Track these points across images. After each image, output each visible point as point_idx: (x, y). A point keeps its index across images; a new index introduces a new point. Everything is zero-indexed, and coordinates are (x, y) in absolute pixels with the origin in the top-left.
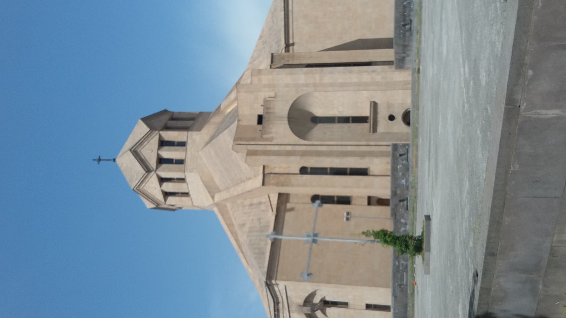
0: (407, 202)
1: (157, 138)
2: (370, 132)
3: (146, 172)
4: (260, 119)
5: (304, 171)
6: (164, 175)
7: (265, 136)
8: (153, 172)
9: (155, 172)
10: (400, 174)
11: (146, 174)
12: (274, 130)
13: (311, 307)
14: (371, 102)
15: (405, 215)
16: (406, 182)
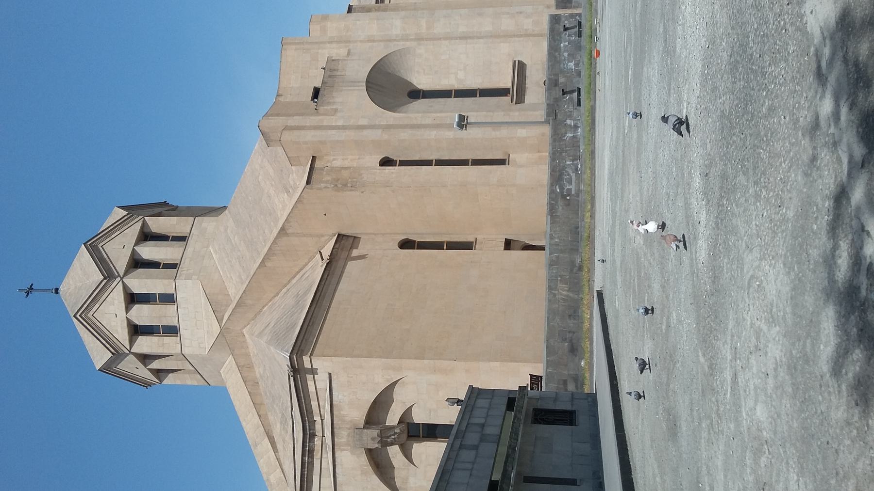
0: (579, 95)
3: (105, 278)
4: (316, 93)
5: (386, 162)
6: (135, 291)
7: (322, 109)
8: (119, 279)
9: (122, 279)
10: (566, 54)
11: (105, 281)
12: (339, 99)
13: (381, 430)
14: (515, 62)
15: (575, 114)
16: (577, 65)
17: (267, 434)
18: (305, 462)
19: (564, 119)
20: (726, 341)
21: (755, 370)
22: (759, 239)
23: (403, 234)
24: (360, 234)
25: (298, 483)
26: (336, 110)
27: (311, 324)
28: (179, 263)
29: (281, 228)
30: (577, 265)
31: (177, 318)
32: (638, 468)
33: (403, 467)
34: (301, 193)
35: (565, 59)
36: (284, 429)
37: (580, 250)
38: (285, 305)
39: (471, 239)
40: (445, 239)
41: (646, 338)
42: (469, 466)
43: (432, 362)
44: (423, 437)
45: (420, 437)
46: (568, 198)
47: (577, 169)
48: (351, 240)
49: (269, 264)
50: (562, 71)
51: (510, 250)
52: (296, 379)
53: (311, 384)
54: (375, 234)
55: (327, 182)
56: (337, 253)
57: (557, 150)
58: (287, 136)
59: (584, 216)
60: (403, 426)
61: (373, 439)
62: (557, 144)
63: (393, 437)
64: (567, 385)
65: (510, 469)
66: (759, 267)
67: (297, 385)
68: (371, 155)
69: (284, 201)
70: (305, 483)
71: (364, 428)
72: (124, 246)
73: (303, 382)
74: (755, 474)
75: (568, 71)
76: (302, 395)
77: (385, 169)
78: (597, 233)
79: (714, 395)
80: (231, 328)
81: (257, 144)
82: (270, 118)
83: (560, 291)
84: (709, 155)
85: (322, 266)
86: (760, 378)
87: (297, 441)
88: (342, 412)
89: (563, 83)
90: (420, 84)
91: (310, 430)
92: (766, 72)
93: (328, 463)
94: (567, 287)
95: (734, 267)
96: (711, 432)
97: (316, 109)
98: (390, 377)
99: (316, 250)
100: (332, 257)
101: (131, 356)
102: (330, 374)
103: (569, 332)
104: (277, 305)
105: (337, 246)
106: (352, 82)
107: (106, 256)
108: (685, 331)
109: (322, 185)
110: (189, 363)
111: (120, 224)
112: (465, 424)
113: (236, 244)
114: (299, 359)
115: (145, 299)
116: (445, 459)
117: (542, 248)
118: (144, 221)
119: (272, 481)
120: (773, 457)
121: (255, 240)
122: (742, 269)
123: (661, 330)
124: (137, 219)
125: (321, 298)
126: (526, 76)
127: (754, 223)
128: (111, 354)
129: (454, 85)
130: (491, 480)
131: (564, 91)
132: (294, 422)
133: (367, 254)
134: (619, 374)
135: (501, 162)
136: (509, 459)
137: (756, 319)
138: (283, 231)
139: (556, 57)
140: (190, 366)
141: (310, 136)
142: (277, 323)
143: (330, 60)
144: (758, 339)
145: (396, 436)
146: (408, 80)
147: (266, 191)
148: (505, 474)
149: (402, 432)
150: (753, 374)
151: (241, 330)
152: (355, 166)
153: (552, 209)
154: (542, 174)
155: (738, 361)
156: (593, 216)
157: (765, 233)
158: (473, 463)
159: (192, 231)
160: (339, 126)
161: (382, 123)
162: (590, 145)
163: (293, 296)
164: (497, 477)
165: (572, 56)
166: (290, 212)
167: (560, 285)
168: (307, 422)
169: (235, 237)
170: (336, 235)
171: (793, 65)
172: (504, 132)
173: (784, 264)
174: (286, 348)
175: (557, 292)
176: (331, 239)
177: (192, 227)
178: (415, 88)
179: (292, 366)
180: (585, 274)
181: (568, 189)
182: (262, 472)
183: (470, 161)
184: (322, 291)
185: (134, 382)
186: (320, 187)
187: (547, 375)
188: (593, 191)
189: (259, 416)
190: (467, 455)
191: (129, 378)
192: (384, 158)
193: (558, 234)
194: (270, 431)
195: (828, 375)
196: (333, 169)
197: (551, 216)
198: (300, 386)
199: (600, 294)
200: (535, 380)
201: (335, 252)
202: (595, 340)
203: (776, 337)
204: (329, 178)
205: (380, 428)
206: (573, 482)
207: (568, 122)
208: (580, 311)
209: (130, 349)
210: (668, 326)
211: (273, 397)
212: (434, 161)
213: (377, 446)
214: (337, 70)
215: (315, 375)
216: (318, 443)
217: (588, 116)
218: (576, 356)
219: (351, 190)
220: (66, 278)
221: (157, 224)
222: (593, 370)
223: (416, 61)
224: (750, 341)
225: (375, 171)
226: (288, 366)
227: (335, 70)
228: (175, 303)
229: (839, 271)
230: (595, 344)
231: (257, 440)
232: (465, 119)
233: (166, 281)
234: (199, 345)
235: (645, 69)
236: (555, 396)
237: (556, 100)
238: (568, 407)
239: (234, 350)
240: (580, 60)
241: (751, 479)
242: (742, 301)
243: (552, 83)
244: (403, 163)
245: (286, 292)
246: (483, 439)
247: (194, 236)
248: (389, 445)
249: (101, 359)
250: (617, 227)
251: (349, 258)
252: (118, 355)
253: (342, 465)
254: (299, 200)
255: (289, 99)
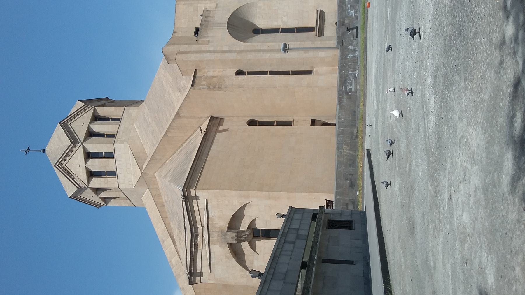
0: (357, 31)
1: (91, 112)
2: (316, 35)
3: (72, 143)
4: (197, 31)
5: (239, 73)
6: (91, 150)
7: (200, 40)
9: (82, 144)
10: (349, 6)
11: (72, 145)
13: (237, 233)
14: (318, 11)
15: (355, 43)
16: (356, 12)
17: (170, 235)
18: (193, 252)
19: (348, 46)
20: (445, 176)
21: (462, 192)
22: (467, 114)
23: (249, 116)
24: (225, 116)
25: (188, 263)
26: (209, 41)
27: (195, 170)
28: (116, 134)
29: (177, 113)
30: (355, 134)
31: (115, 167)
32: (390, 254)
33: (250, 254)
34: (189, 92)
35: (348, 9)
36: (180, 232)
37: (357, 125)
38: (179, 159)
39: (290, 119)
40: (275, 119)
41: (396, 177)
42: (290, 253)
43: (267, 192)
44: (262, 237)
45: (260, 237)
46: (350, 94)
47: (355, 77)
48: (219, 120)
49: (169, 135)
50: (347, 16)
51: (314, 126)
52: (187, 203)
53: (195, 205)
54: (233, 117)
55: (204, 85)
56: (210, 128)
57: (343, 65)
58: (179, 57)
59: (359, 105)
60: (250, 230)
61: (232, 238)
62: (344, 61)
63: (244, 237)
64: (348, 206)
65: (314, 255)
66: (466, 130)
67: (187, 206)
68: (230, 69)
69: (178, 96)
70: (193, 263)
71: (227, 231)
72: (83, 124)
73: (190, 204)
74: (461, 254)
75: (351, 16)
76: (190, 212)
77: (239, 77)
78: (367, 115)
79: (437, 209)
80: (148, 173)
81: (162, 62)
82: (169, 46)
83: (344, 150)
84: (437, 63)
85: (201, 136)
86: (465, 197)
87: (188, 239)
88: (214, 222)
89: (347, 23)
90: (260, 25)
91: (195, 233)
92: (473, 11)
93: (206, 252)
94: (349, 148)
95: (451, 131)
96: (435, 230)
97: (197, 41)
98: (242, 202)
99: (197, 126)
100: (207, 130)
101: (89, 190)
102: (207, 200)
103: (350, 175)
104: (175, 159)
105: (210, 124)
106: (219, 24)
107: (72, 130)
108: (420, 171)
109: (201, 87)
110: (123, 193)
111: (80, 111)
112: (287, 228)
113: (150, 123)
114: (188, 191)
115: (96, 155)
116: (275, 249)
117: (334, 125)
118: (95, 108)
119: (173, 263)
120: (472, 244)
121: (161, 120)
122: (456, 132)
123: (406, 172)
124: (90, 108)
125: (201, 155)
126: (324, 20)
127: (464, 104)
128: (76, 188)
129: (281, 26)
130: (302, 261)
131: (348, 28)
132: (186, 228)
133: (229, 129)
134: (380, 199)
135: (309, 72)
136: (314, 249)
137: (464, 162)
138: (178, 115)
139: (343, 8)
140: (124, 195)
141: (193, 57)
142: (175, 169)
143: (206, 11)
144: (465, 173)
145: (246, 236)
146: (253, 22)
147: (167, 91)
148: (311, 258)
149: (250, 234)
150: (461, 195)
151: (153, 174)
152: (221, 75)
153: (340, 101)
154: (334, 79)
155: (453, 187)
156: (365, 105)
157: (470, 110)
158: (292, 251)
159: (123, 115)
160: (211, 51)
161: (237, 49)
162: (363, 61)
163: (184, 154)
164: (306, 259)
165: (353, 7)
166: (182, 103)
167: (344, 147)
168: (193, 228)
169: (149, 119)
170: (210, 118)
171: (489, 6)
172: (311, 54)
173: (482, 128)
174: (181, 184)
175: (342, 151)
176: (207, 120)
177: (124, 112)
178: (257, 27)
179: (184, 195)
180: (359, 140)
181: (350, 88)
182: (167, 257)
183: (291, 72)
184: (201, 151)
185: (92, 205)
186: (199, 88)
187: (336, 200)
188: (365, 89)
189: (165, 225)
190: (288, 247)
191: (88, 202)
192: (239, 70)
193: (344, 116)
194: (171, 233)
195: (507, 193)
196: (207, 78)
197: (340, 105)
198: (189, 207)
199: (369, 152)
200: (329, 203)
201: (209, 127)
202: (365, 179)
203: (476, 172)
204: (204, 83)
205: (236, 232)
206: (351, 263)
207: (350, 47)
208: (356, 162)
209: (88, 185)
210: (410, 169)
211: (173, 213)
212: (268, 72)
213: (235, 242)
214: (210, 16)
215: (198, 201)
216: (200, 241)
217: (362, 44)
218: (354, 189)
219: (218, 90)
220: (49, 143)
221: (102, 111)
222: (364, 197)
223: (257, 10)
224: (460, 175)
225: (233, 78)
226: (181, 195)
227: (208, 17)
228: (114, 158)
229: (516, 130)
230: (365, 181)
231: (164, 239)
232: (288, 46)
233: (108, 145)
234: (129, 183)
235: (398, 13)
236: (341, 213)
237: (343, 34)
238: (349, 219)
239: (149, 186)
240: (357, 10)
241: (459, 257)
242: (455, 152)
243: (340, 24)
244: (250, 73)
245: (180, 152)
246: (298, 237)
247: (124, 118)
248: (242, 241)
249: (71, 191)
250: (380, 111)
251: (217, 131)
252: (81, 189)
253: (214, 253)
254: (187, 96)
255: (180, 34)
